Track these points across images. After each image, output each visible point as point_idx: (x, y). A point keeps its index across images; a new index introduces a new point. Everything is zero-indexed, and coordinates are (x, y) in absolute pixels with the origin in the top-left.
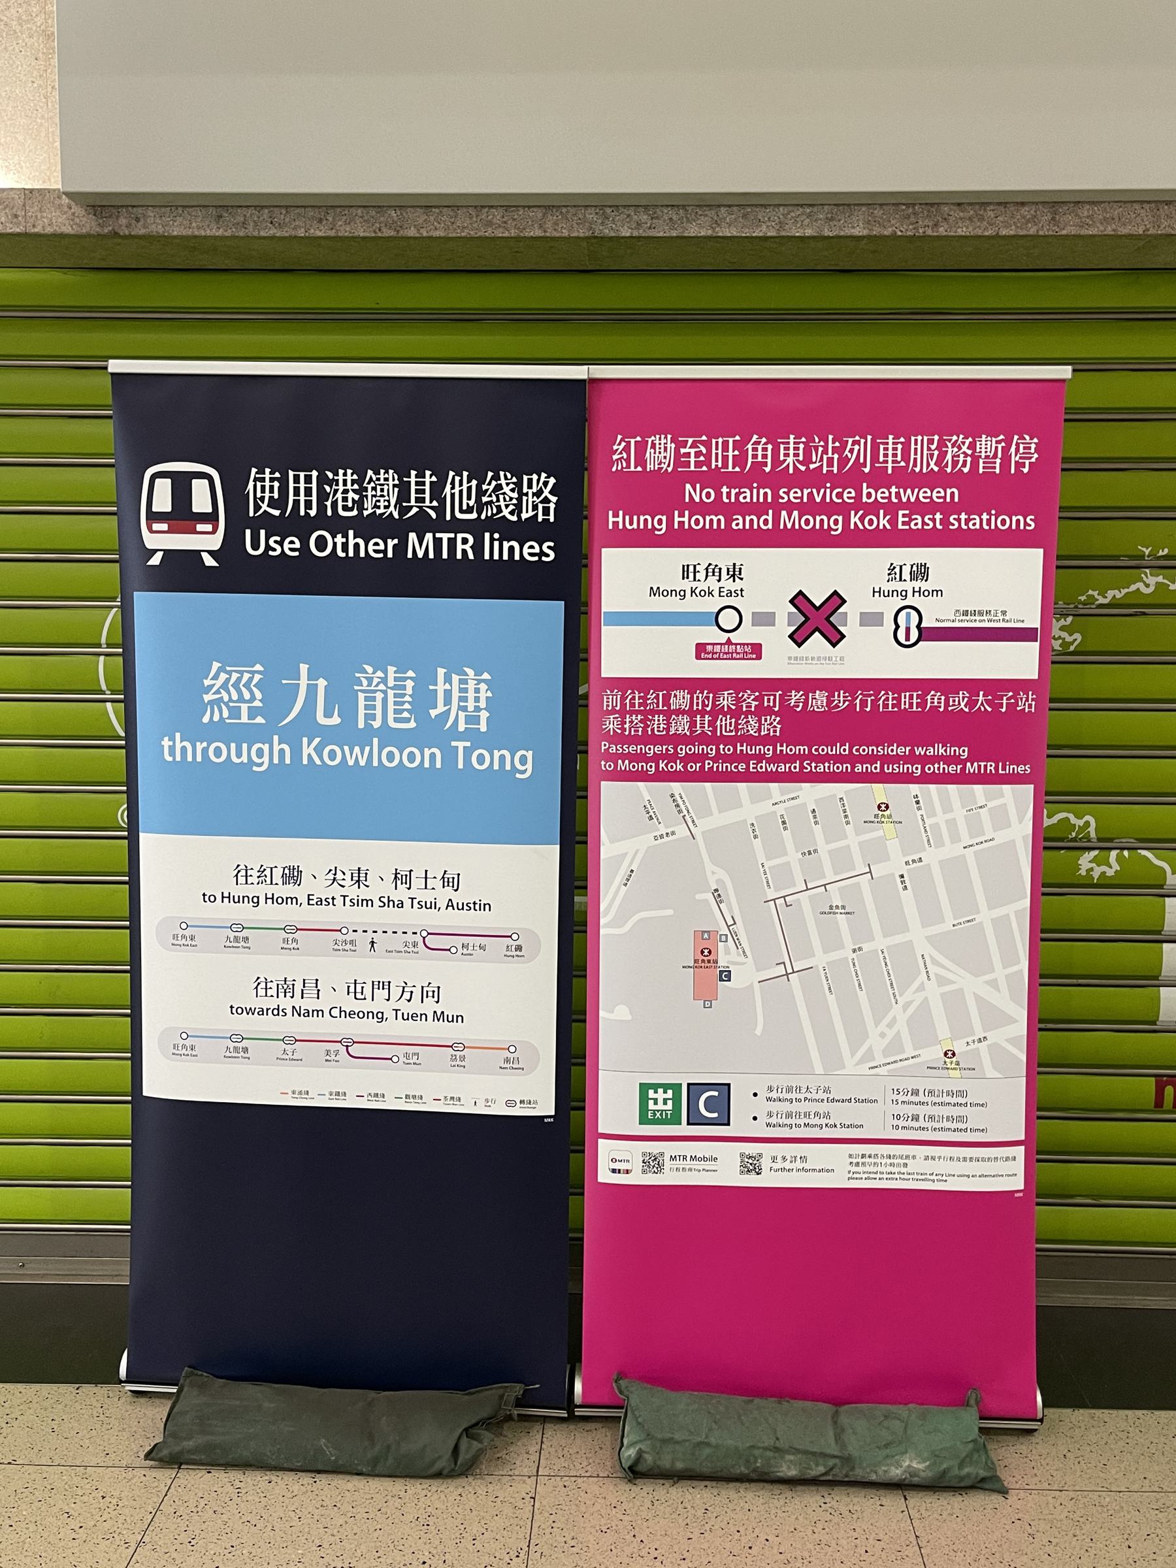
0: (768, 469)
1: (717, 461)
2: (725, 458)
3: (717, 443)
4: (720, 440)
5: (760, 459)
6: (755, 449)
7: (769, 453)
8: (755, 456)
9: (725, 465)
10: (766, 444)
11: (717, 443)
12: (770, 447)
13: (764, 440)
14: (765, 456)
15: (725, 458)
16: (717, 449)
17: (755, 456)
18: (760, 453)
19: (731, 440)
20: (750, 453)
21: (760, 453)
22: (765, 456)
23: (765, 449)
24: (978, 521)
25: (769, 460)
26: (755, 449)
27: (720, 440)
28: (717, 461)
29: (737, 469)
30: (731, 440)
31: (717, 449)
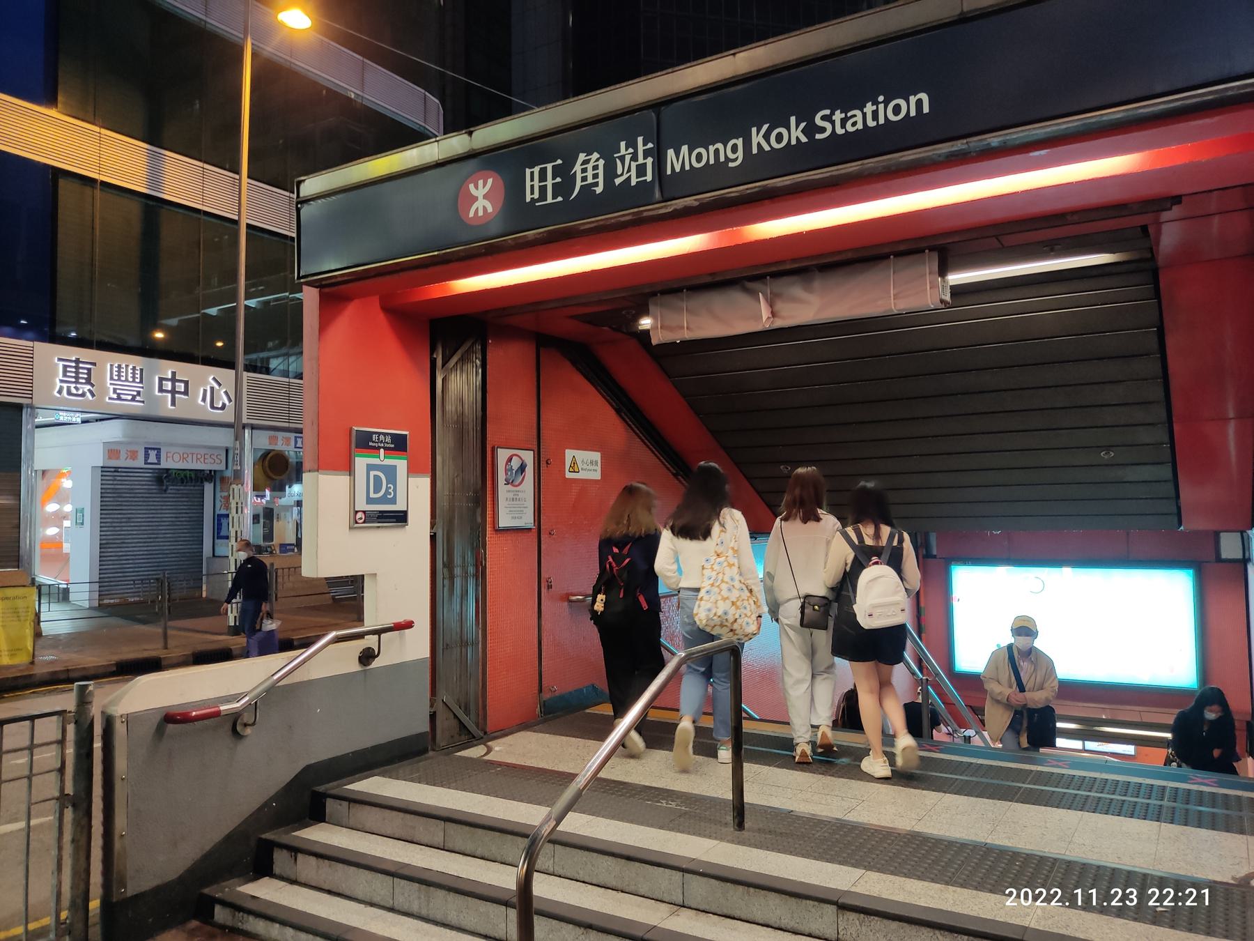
0: (599, 190)
1: (532, 193)
2: (543, 190)
3: (532, 173)
4: (536, 170)
5: (590, 180)
6: (584, 171)
7: (601, 171)
8: (584, 179)
9: (543, 196)
10: (597, 160)
11: (532, 173)
12: (601, 162)
13: (596, 155)
14: (595, 176)
15: (543, 190)
16: (532, 180)
17: (584, 179)
18: (590, 173)
19: (549, 166)
21: (590, 173)
22: (595, 176)
23: (595, 168)
24: (859, 118)
25: (601, 180)
26: (584, 171)
27: (536, 170)
28: (532, 193)
29: (560, 199)
30: (549, 166)
31: (532, 180)
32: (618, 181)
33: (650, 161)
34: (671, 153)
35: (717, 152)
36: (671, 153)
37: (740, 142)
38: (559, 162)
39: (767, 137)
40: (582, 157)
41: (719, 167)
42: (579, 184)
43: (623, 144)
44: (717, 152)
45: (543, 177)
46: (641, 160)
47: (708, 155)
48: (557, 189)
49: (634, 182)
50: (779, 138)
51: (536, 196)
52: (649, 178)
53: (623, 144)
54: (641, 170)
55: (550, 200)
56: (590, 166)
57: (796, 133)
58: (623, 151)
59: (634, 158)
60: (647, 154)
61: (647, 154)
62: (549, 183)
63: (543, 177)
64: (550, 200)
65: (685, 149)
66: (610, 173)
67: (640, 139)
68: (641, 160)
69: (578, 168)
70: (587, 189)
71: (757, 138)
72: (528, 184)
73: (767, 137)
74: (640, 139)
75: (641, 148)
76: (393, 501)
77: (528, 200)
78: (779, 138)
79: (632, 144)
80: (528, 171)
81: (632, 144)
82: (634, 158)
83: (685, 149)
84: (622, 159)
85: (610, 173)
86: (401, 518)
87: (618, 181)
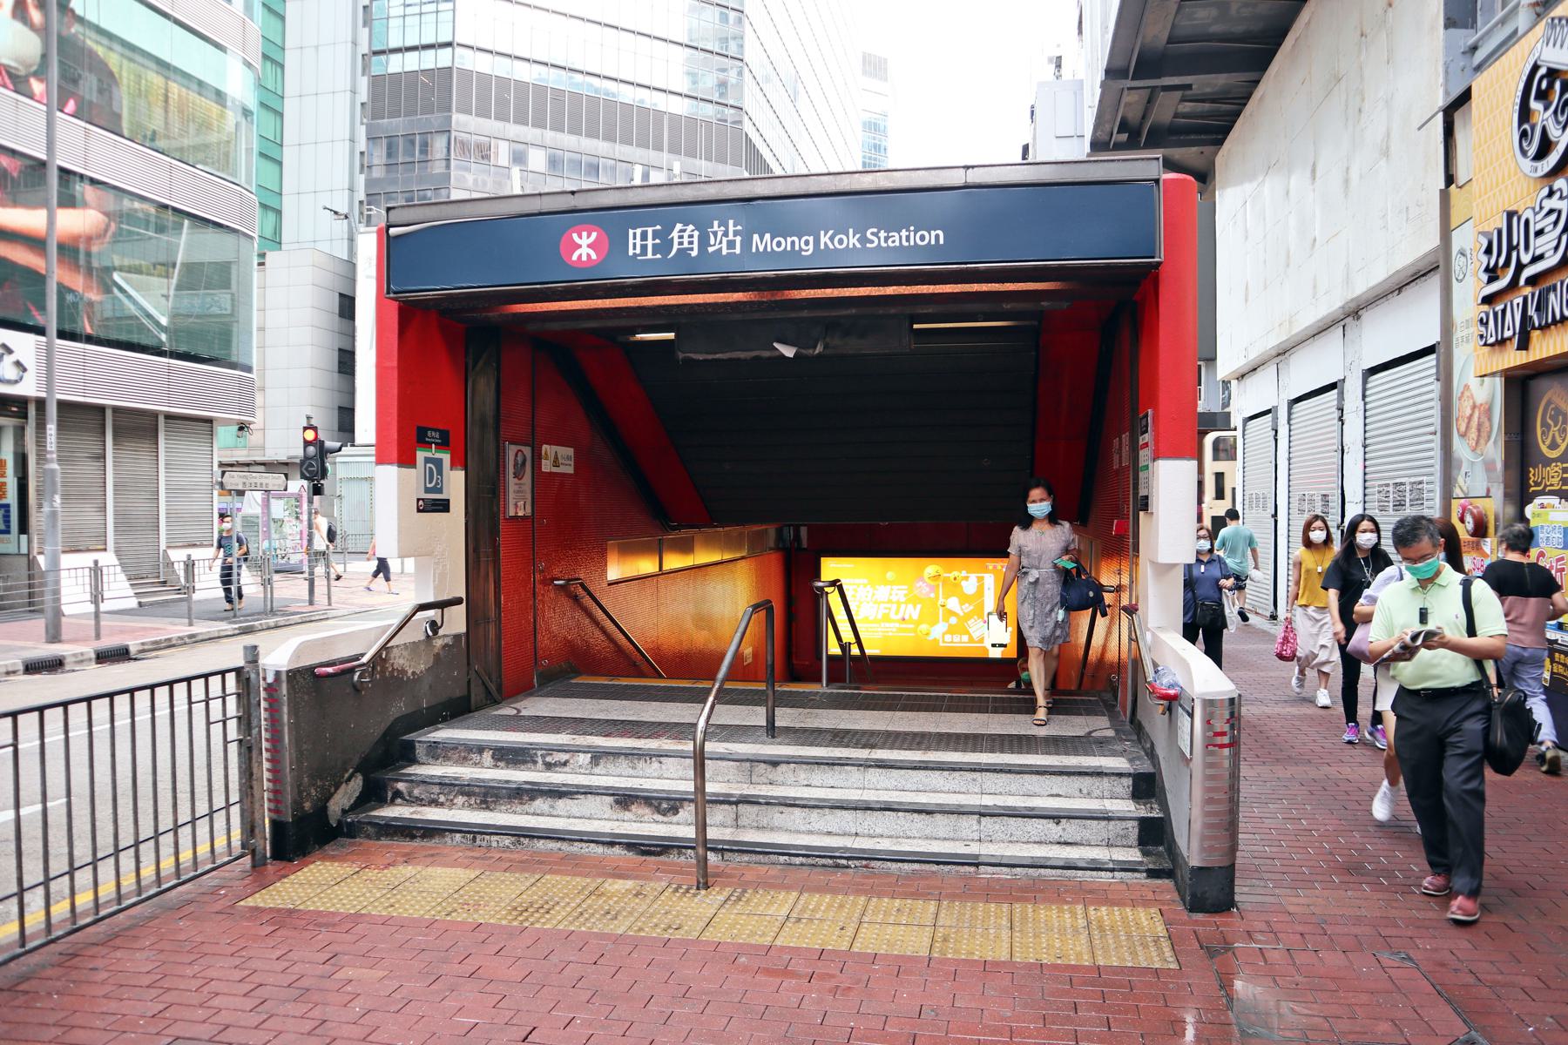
0: (694, 253)
2: (644, 248)
4: (639, 231)
5: (686, 245)
7: (695, 240)
8: (681, 243)
12: (696, 233)
13: (691, 227)
14: (691, 243)
15: (644, 248)
17: (681, 243)
18: (686, 240)
19: (650, 230)
20: (676, 241)
21: (686, 240)
22: (691, 243)
25: (695, 246)
27: (639, 231)
32: (711, 249)
33: (738, 239)
34: (756, 237)
35: (793, 243)
36: (756, 237)
37: (811, 239)
39: (832, 239)
40: (679, 226)
41: (795, 254)
42: (676, 247)
43: (716, 223)
44: (793, 243)
45: (644, 236)
46: (731, 237)
47: (786, 244)
48: (656, 249)
49: (725, 252)
50: (841, 241)
51: (638, 251)
52: (738, 251)
53: (716, 223)
54: (731, 244)
55: (650, 256)
56: (686, 235)
57: (853, 241)
58: (716, 228)
59: (726, 234)
60: (736, 233)
62: (650, 242)
63: (644, 236)
64: (650, 256)
65: (768, 236)
66: (704, 242)
67: (731, 222)
68: (731, 237)
69: (675, 234)
71: (824, 239)
72: (631, 241)
73: (832, 239)
74: (731, 222)
75: (731, 229)
76: (440, 491)
77: (631, 252)
78: (841, 241)
79: (724, 224)
80: (631, 232)
81: (724, 224)
82: (726, 234)
83: (768, 236)
84: (715, 234)
85: (704, 242)
86: (443, 506)
87: (711, 249)
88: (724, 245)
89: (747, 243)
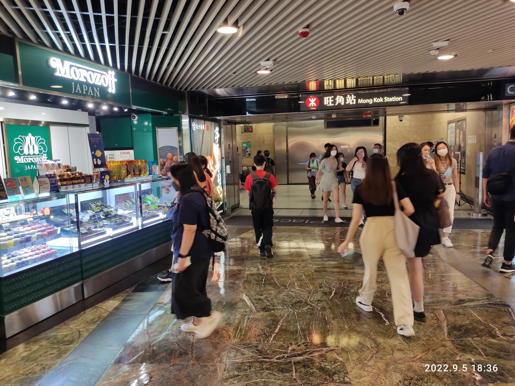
0: (343, 104)
2: (329, 102)
5: (340, 102)
12: (343, 99)
15: (329, 102)
18: (340, 100)
19: (330, 98)
21: (340, 100)
27: (327, 98)
32: (347, 103)
33: (355, 100)
38: (333, 97)
41: (368, 104)
45: (329, 99)
46: (353, 99)
48: (332, 103)
54: (353, 101)
59: (351, 99)
61: (354, 98)
63: (329, 99)
64: (330, 104)
69: (337, 99)
70: (339, 104)
77: (325, 104)
80: (325, 98)
81: (351, 95)
82: (351, 99)
88: (351, 102)
89: (357, 101)
